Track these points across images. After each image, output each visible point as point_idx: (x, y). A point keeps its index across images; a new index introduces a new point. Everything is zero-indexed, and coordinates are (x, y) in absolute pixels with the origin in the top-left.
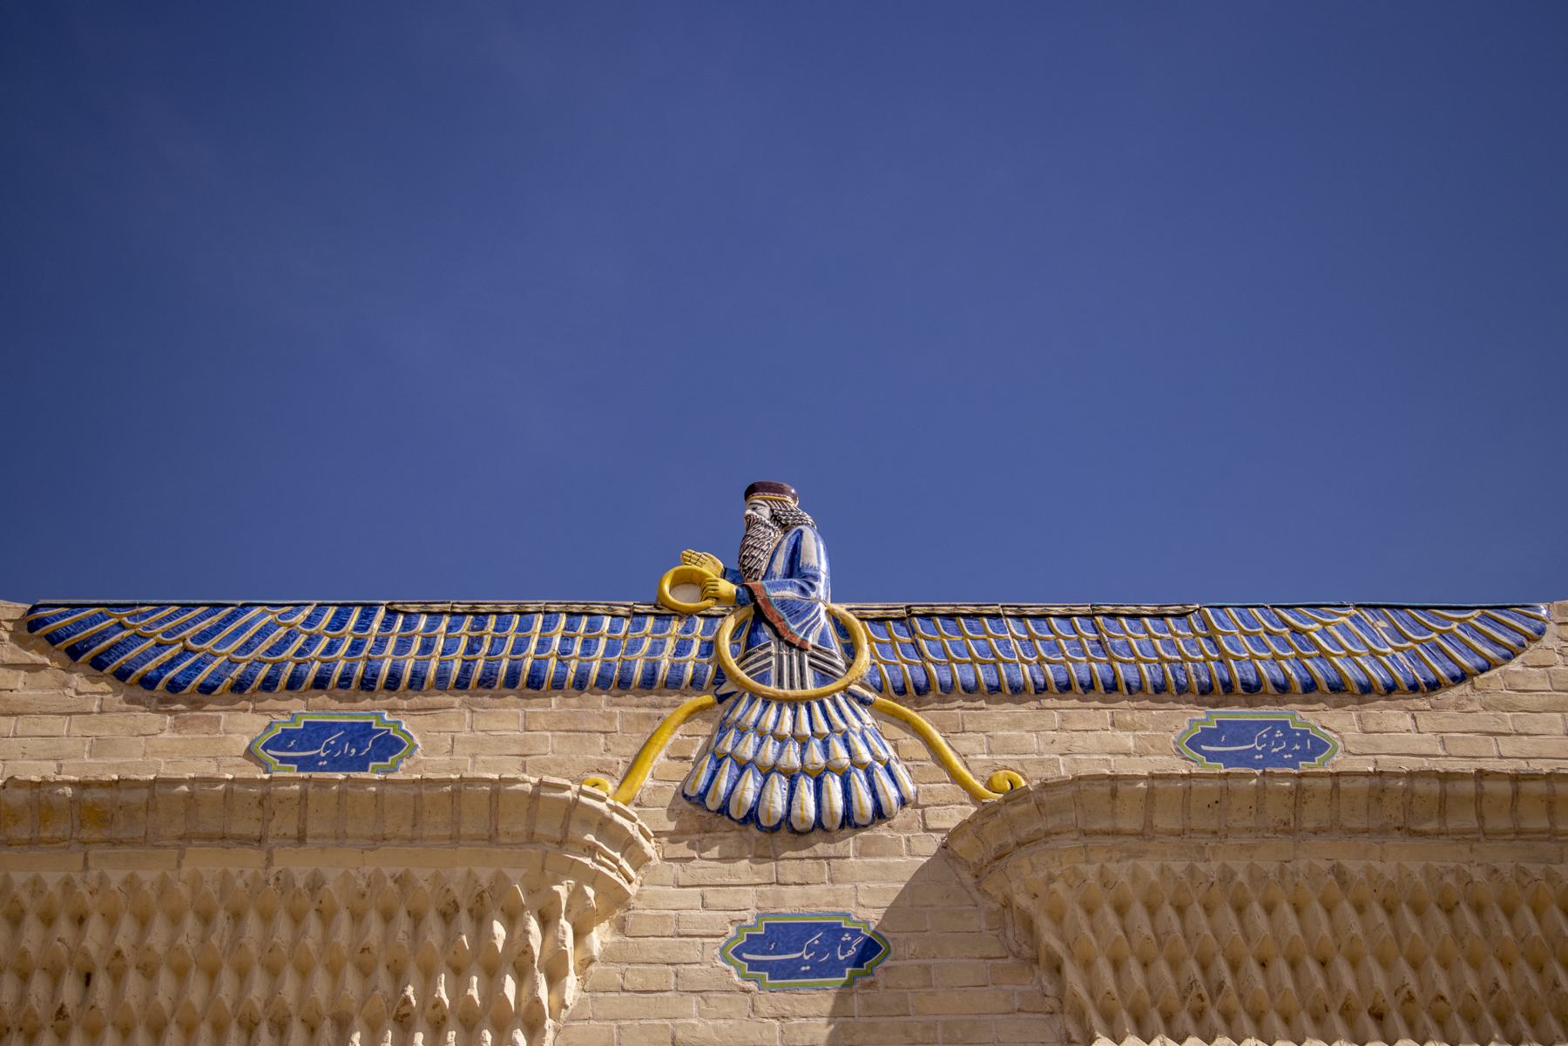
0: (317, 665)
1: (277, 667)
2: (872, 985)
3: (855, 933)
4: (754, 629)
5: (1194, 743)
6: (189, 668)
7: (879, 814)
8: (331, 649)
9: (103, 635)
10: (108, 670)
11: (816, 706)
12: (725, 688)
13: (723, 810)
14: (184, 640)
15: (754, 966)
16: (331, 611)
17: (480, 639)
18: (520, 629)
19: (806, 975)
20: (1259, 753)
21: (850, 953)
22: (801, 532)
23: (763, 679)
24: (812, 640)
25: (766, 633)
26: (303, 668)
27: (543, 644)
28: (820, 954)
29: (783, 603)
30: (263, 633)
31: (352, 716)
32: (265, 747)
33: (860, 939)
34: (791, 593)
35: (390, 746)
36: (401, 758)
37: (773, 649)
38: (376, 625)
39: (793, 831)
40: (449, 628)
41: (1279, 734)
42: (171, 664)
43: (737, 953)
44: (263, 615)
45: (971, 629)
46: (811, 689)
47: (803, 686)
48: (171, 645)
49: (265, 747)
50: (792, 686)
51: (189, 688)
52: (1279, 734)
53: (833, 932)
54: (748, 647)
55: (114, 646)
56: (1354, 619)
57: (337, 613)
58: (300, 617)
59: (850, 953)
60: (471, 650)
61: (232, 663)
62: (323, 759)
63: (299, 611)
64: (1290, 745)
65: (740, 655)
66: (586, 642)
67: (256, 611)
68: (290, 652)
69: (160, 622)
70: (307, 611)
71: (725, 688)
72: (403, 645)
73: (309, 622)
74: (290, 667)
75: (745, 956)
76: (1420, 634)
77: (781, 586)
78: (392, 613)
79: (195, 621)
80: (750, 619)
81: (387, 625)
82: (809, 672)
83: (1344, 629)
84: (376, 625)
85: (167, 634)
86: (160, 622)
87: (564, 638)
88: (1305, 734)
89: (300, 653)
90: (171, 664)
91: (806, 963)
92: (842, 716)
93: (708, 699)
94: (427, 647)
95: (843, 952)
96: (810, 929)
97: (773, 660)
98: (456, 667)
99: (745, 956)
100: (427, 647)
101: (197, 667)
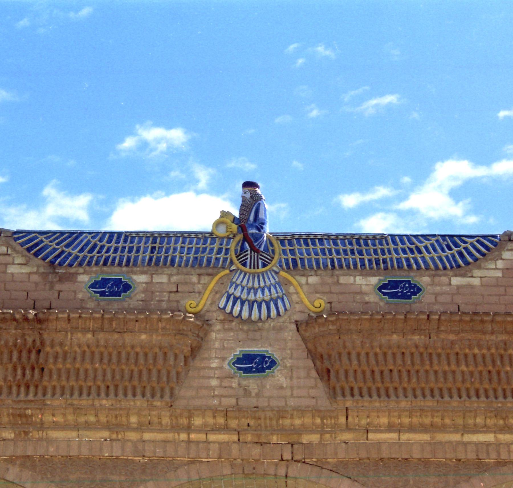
0: (104, 257)
1: (92, 258)
2: (273, 376)
3: (269, 358)
4: (243, 244)
5: (380, 289)
6: (64, 258)
7: (278, 314)
8: (107, 252)
9: (37, 245)
10: (40, 257)
11: (261, 278)
12: (233, 268)
13: (231, 312)
14: (61, 247)
15: (239, 369)
16: (107, 235)
17: (155, 247)
18: (168, 244)
19: (254, 372)
20: (400, 292)
21: (267, 365)
22: (259, 204)
23: (244, 265)
24: (262, 249)
25: (247, 245)
26: (100, 258)
27: (175, 249)
28: (258, 366)
29: (252, 234)
30: (87, 244)
31: (115, 276)
32: (89, 287)
33: (270, 360)
34: (254, 231)
35: (127, 287)
36: (131, 292)
37: (249, 252)
38: (122, 241)
39: (252, 321)
40: (145, 243)
41: (407, 285)
42: (59, 256)
43: (234, 364)
44: (86, 237)
45: (312, 244)
46: (261, 270)
47: (258, 268)
48: (58, 249)
49: (89, 287)
50: (254, 268)
51: (65, 265)
52: (407, 285)
53: (263, 357)
54: (241, 251)
55: (41, 249)
56: (437, 241)
57: (110, 236)
58: (98, 238)
59: (267, 365)
60: (152, 252)
61: (77, 257)
62: (107, 292)
63: (97, 235)
64: (410, 290)
65: (238, 254)
66: (188, 248)
67: (85, 235)
68: (96, 251)
69: (54, 240)
70: (100, 235)
71: (233, 268)
72: (130, 250)
73: (100, 240)
74: (95, 259)
75: (236, 365)
76: (456, 247)
77: (251, 226)
78: (126, 237)
79: (65, 239)
80: (242, 239)
81: (125, 241)
82: (260, 261)
83: (432, 245)
84: (122, 241)
85: (58, 244)
86: (54, 240)
87: (182, 247)
88: (415, 285)
89: (98, 252)
90: (59, 256)
91: (254, 368)
92: (269, 279)
93: (227, 271)
94: (138, 251)
95: (266, 364)
96: (255, 356)
97: (249, 256)
98: (147, 258)
99: (236, 365)
100: (138, 251)
101: (66, 258)
